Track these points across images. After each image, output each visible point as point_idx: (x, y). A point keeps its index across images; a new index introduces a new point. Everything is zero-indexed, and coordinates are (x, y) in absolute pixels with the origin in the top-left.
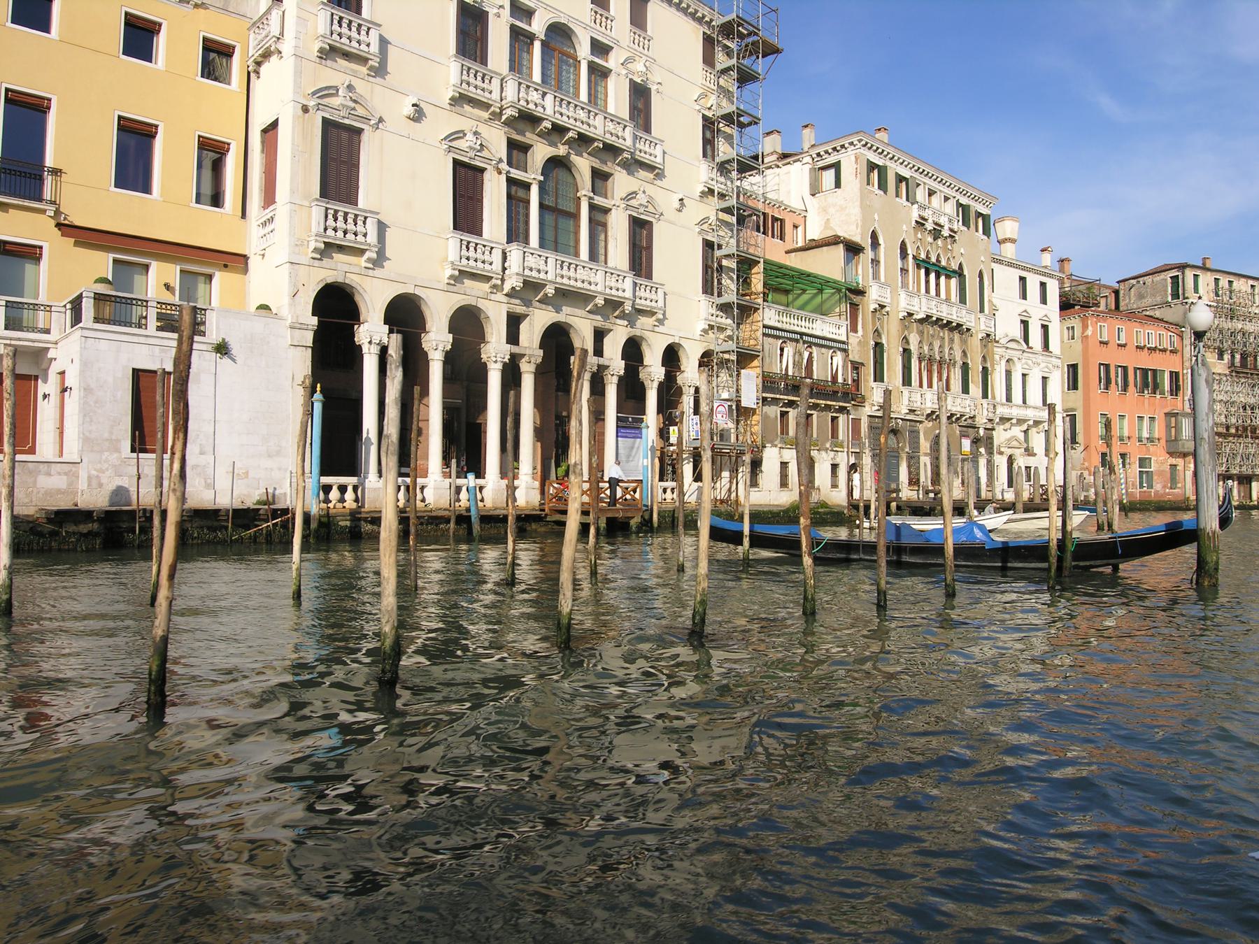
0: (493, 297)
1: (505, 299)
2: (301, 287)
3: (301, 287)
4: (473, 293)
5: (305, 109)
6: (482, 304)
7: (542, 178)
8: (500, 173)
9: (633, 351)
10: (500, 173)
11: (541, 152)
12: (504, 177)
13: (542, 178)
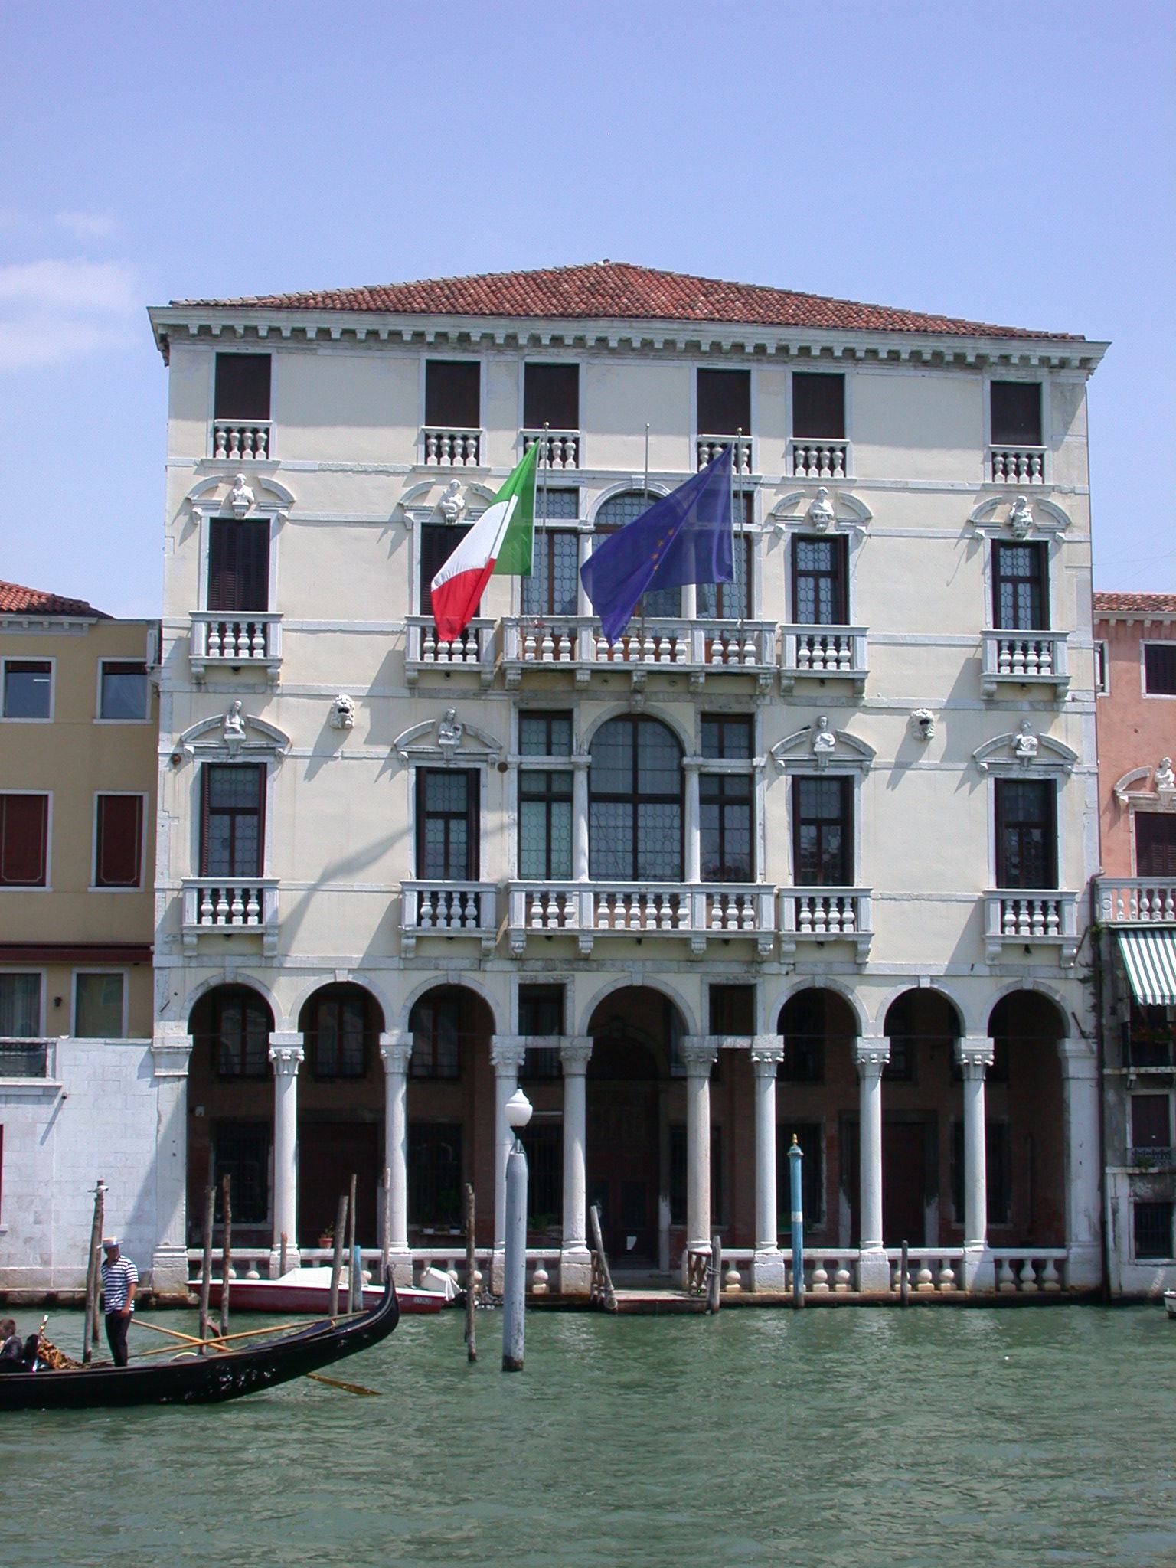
0: (489, 966)
1: (509, 966)
2: (173, 998)
3: (173, 998)
4: (454, 968)
5: (176, 760)
6: (471, 980)
7: (589, 758)
8: (503, 767)
9: (817, 1019)
10: (503, 767)
11: (588, 718)
12: (512, 775)
13: (589, 758)
